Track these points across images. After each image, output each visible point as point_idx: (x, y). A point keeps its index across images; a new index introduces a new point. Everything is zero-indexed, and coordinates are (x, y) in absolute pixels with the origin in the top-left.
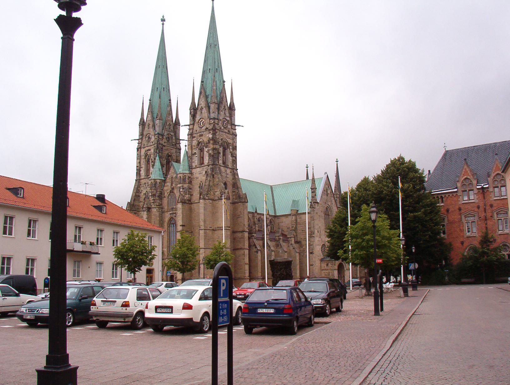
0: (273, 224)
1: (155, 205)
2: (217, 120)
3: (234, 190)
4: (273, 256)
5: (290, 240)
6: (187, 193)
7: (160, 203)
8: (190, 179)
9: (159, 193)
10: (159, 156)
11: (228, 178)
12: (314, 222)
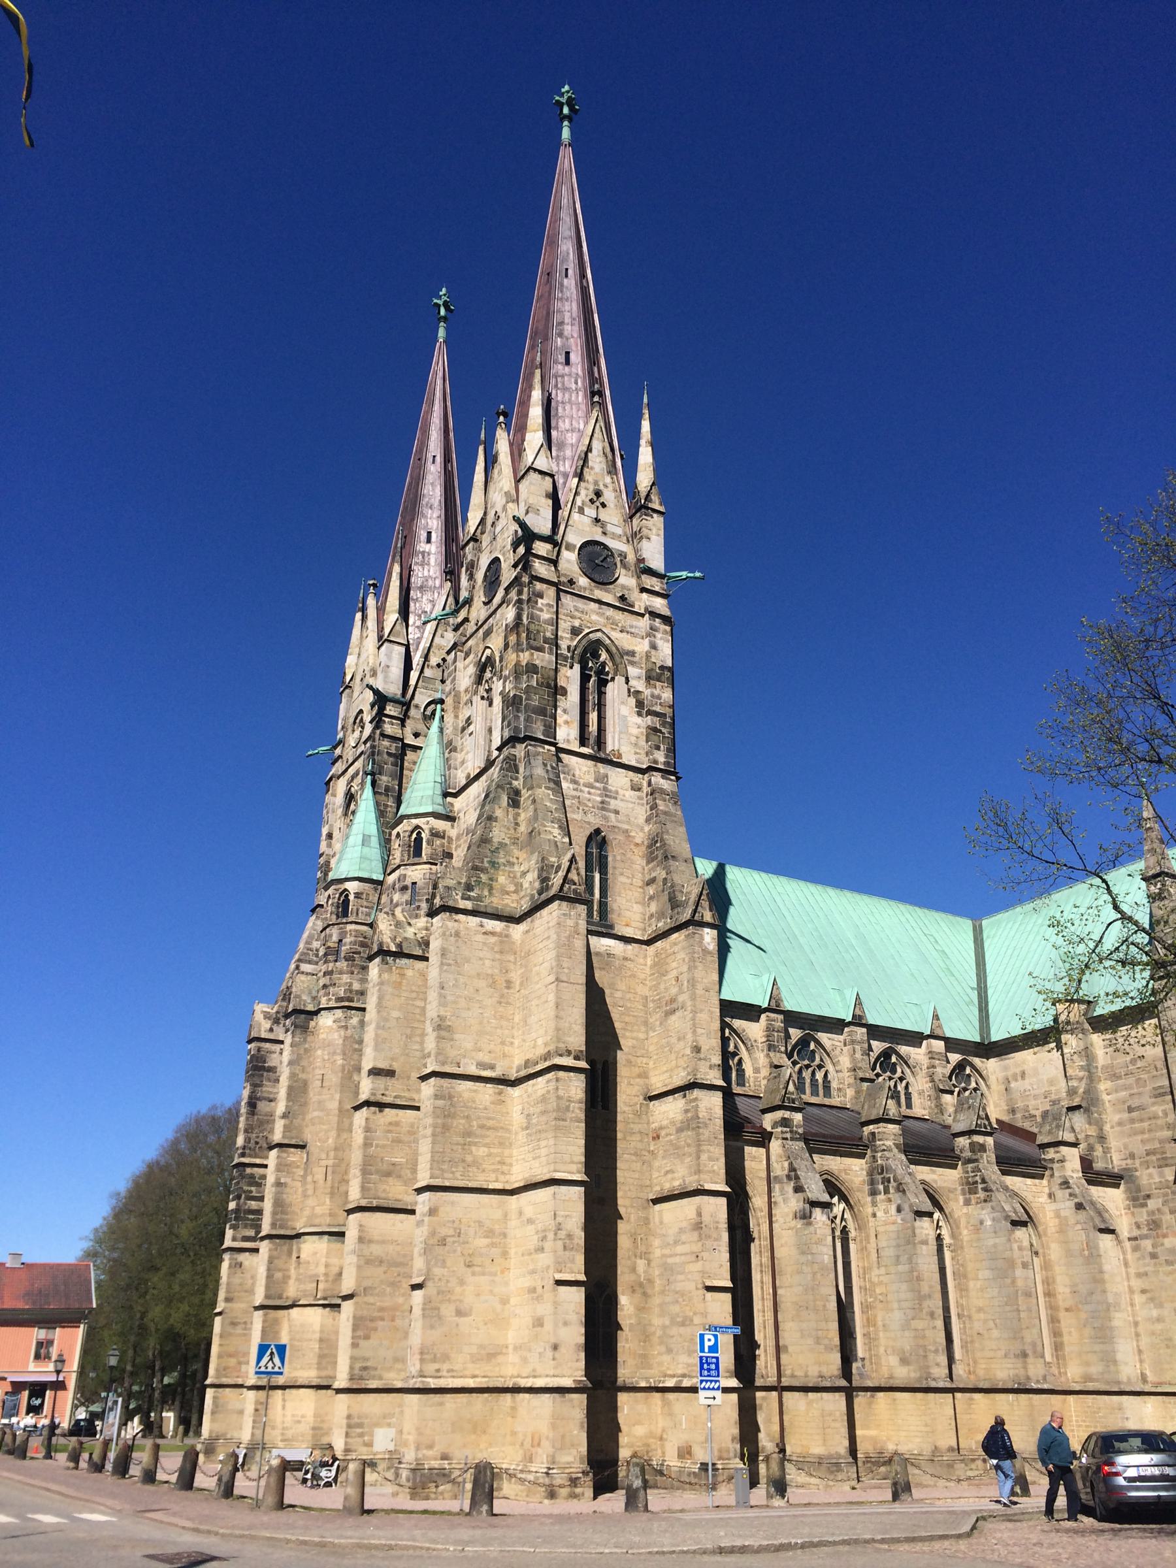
0: (975, 1090)
1: (330, 1000)
2: (549, 546)
3: (653, 875)
4: (925, 1242)
5: (1052, 1161)
6: (418, 908)
7: (356, 986)
8: (438, 842)
9: (351, 943)
10: (374, 784)
11: (617, 812)
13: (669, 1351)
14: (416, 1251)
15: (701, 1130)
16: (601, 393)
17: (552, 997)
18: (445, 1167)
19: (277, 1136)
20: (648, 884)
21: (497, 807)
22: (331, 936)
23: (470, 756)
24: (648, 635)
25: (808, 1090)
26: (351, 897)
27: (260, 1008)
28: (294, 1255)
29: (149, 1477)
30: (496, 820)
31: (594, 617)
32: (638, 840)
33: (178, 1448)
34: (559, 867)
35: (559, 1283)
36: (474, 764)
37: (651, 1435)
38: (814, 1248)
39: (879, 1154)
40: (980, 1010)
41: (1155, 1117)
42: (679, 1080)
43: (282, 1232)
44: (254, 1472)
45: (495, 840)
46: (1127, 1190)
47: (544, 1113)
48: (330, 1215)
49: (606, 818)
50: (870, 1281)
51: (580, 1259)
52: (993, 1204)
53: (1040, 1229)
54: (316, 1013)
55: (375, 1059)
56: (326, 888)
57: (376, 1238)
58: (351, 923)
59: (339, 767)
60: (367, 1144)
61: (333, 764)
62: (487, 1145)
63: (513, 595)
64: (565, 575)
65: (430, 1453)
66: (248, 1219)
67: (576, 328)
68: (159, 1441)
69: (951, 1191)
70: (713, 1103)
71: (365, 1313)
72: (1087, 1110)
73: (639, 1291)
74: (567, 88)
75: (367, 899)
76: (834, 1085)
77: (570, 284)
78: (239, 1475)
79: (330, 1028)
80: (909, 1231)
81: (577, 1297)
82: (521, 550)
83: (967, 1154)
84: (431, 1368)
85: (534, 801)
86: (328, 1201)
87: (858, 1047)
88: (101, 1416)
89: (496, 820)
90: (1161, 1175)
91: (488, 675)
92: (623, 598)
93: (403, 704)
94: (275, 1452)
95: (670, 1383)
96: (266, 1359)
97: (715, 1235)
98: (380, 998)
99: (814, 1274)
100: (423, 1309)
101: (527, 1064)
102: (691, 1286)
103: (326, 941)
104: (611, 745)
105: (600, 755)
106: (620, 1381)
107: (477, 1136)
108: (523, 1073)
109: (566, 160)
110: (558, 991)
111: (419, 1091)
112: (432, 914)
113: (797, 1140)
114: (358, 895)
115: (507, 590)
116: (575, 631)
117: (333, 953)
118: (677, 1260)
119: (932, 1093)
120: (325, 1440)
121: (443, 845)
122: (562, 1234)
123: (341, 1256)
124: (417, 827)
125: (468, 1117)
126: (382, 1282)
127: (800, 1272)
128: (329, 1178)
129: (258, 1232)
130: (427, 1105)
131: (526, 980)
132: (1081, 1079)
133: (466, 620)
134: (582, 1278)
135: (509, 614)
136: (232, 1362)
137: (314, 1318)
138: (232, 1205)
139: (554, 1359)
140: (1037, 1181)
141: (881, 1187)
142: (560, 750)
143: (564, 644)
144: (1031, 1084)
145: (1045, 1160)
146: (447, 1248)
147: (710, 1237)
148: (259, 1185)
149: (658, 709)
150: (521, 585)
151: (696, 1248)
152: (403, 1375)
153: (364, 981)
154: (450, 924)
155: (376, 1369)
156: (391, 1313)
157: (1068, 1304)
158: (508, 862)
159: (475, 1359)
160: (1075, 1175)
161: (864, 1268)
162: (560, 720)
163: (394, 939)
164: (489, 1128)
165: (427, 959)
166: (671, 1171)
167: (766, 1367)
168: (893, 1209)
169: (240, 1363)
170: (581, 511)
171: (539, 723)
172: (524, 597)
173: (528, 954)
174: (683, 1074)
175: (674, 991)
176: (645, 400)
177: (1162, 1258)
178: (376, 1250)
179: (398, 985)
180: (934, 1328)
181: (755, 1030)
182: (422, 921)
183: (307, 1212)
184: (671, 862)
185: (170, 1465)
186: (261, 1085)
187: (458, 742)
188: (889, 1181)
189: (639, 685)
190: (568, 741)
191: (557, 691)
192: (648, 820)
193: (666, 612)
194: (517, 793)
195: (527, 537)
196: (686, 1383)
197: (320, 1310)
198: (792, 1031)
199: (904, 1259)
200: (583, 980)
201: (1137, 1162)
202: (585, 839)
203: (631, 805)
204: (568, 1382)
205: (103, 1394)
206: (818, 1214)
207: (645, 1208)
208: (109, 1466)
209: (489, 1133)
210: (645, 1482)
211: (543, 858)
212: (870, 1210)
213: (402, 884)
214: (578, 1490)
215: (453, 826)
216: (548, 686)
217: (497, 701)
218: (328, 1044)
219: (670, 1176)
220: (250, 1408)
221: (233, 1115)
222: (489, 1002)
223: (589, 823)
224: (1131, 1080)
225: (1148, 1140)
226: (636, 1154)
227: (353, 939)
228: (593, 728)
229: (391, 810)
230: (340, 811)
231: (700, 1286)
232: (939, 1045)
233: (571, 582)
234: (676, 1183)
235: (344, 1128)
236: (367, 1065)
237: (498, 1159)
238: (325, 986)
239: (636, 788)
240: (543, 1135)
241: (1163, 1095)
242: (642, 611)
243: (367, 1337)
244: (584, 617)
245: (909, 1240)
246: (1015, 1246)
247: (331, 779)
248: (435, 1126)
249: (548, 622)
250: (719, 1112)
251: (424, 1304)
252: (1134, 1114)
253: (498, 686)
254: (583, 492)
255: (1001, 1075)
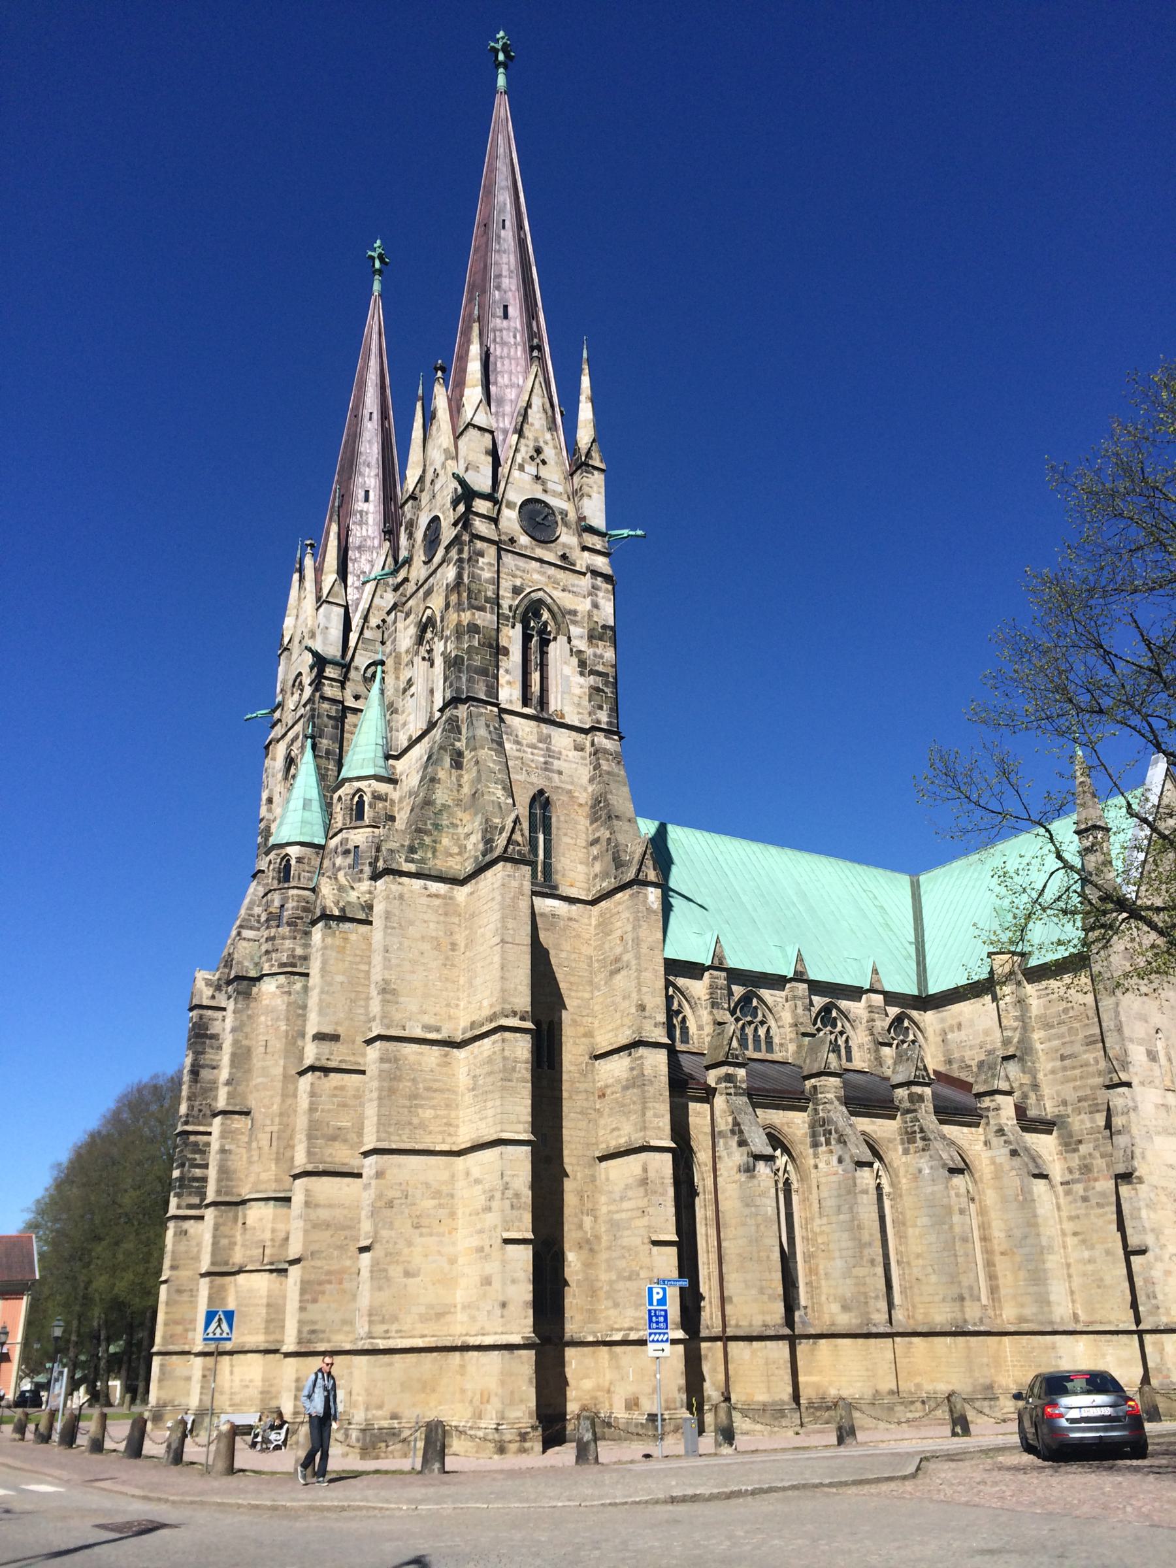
0: (913, 1042)
1: (272, 966)
2: (489, 504)
3: (597, 835)
4: (866, 1192)
5: (988, 1109)
6: (361, 871)
7: (299, 951)
8: (380, 805)
10: (314, 747)
11: (560, 773)
12: (1117, 1005)
13: (616, 1305)
14: (364, 1213)
15: (646, 1088)
16: (540, 348)
17: (497, 959)
18: (391, 1130)
19: (221, 1103)
20: (592, 844)
21: (439, 768)
22: (272, 901)
23: (412, 717)
24: (590, 594)
25: (751, 1046)
26: (293, 862)
27: (201, 975)
28: (240, 1222)
29: (97, 1446)
30: (439, 781)
31: (536, 576)
32: (582, 801)
33: (126, 1416)
34: (503, 829)
35: (507, 1241)
36: (416, 725)
37: (599, 1388)
38: (758, 1201)
39: (821, 1107)
40: (918, 964)
41: (1087, 1065)
42: (624, 1039)
43: (227, 1199)
44: (203, 1438)
45: (439, 802)
46: (1060, 1136)
47: (490, 1074)
48: (276, 1180)
49: (550, 779)
50: (812, 1231)
51: (527, 1217)
52: (932, 1152)
53: (977, 1176)
54: (259, 979)
55: (319, 1023)
56: (267, 853)
57: (322, 1202)
58: (293, 888)
59: (278, 731)
60: (312, 1109)
61: (273, 727)
62: (433, 1107)
63: (454, 554)
64: (506, 534)
65: (379, 1413)
66: (192, 1187)
67: (514, 281)
68: (106, 1410)
69: (890, 1141)
70: (658, 1061)
71: (313, 1277)
72: (1021, 1060)
73: (587, 1247)
74: (501, 34)
75: (309, 864)
76: (776, 1040)
77: (508, 235)
78: (188, 1440)
79: (274, 994)
80: (850, 1182)
81: (524, 1255)
82: (461, 508)
83: (906, 1105)
84: (379, 1329)
85: (477, 762)
86: (273, 1166)
87: (799, 1003)
88: (47, 1386)
89: (439, 781)
90: (1093, 1120)
91: (429, 635)
92: (564, 557)
93: (343, 666)
94: (223, 1418)
95: (618, 1337)
96: (214, 1325)
97: (660, 1190)
98: (324, 963)
99: (758, 1226)
100: (372, 1272)
101: (473, 1025)
102: (638, 1241)
103: (267, 906)
104: (554, 704)
105: (543, 716)
106: (567, 1337)
107: (423, 1099)
108: (468, 1035)
109: (502, 108)
110: (503, 952)
111: (364, 1055)
112: (375, 877)
113: (741, 1095)
114: (299, 860)
115: (448, 548)
116: (516, 591)
117: (275, 919)
118: (624, 1215)
119: (872, 1045)
120: (274, 1404)
121: (385, 808)
122: (509, 1193)
123: (287, 1220)
124: (359, 790)
125: (414, 1080)
126: (329, 1246)
127: (744, 1224)
128: (274, 1143)
129: (202, 1200)
130: (372, 1069)
131: (470, 942)
132: (1015, 1029)
133: (406, 580)
134: (530, 1236)
135: (449, 573)
136: (179, 1329)
137: (260, 1283)
138: (176, 1174)
139: (502, 1317)
140: (973, 1129)
141: (823, 1139)
142: (503, 711)
143: (505, 604)
144: (967, 1035)
145: (981, 1108)
146: (394, 1210)
147: (656, 1192)
148: (203, 1152)
149: (600, 668)
150: (462, 543)
151: (643, 1203)
152: (351, 1337)
153: (307, 946)
154: (394, 887)
155: (323, 1332)
156: (337, 1276)
157: (1003, 1247)
158: (452, 824)
159: (424, 1319)
160: (1010, 1123)
161: (806, 1219)
162: (502, 681)
163: (337, 903)
164: (436, 1091)
165: (370, 923)
166: (617, 1129)
167: (711, 1318)
168: (835, 1159)
169: (186, 1330)
170: (521, 468)
171: (481, 684)
172: (465, 556)
173: (473, 916)
174: (628, 1032)
175: (619, 950)
176: (585, 355)
177: (1094, 1201)
178: (323, 1214)
179: (341, 950)
180: (875, 1274)
181: (698, 988)
182: (365, 885)
183: (252, 1179)
184: (615, 822)
185: (118, 1433)
186: (203, 1053)
187: (399, 704)
188: (830, 1133)
189: (581, 644)
190: (511, 702)
191: (499, 651)
192: (591, 780)
193: (607, 570)
194: (460, 754)
195: (467, 494)
196: (633, 1336)
197: (266, 1275)
198: (734, 988)
199: (845, 1208)
200: (528, 940)
201: (1070, 1109)
202: (528, 800)
203: (574, 766)
204: (516, 1339)
205: (48, 1365)
206: (762, 1167)
207: (591, 1166)
208: (56, 1437)
209: (434, 1095)
210: (594, 1433)
211: (487, 821)
212: (812, 1162)
213: (345, 847)
214: (527, 1445)
215: (395, 789)
216: (490, 646)
217: (439, 661)
218: (270, 1010)
219: (616, 1133)
220: (197, 1374)
221: (176, 1083)
222: (433, 965)
223: (532, 784)
224: (1064, 1029)
225: (1080, 1087)
226: (582, 1113)
227: (295, 904)
228: (535, 688)
229: (332, 774)
230: (280, 776)
231: (647, 1241)
232: (878, 999)
233: (512, 541)
234: (622, 1141)
235: (289, 1094)
236: (311, 1030)
237: (445, 1120)
238: (267, 952)
239: (579, 748)
240: (490, 1096)
241: (1094, 1042)
242: (584, 570)
243: (315, 1301)
244: (525, 576)
245: (850, 1190)
246: (953, 1193)
247: (270, 743)
248: (381, 1089)
249: (488, 581)
250: (664, 1069)
251: (372, 1266)
252: (1067, 1062)
253: (439, 647)
254: (523, 449)
255: (938, 1027)
